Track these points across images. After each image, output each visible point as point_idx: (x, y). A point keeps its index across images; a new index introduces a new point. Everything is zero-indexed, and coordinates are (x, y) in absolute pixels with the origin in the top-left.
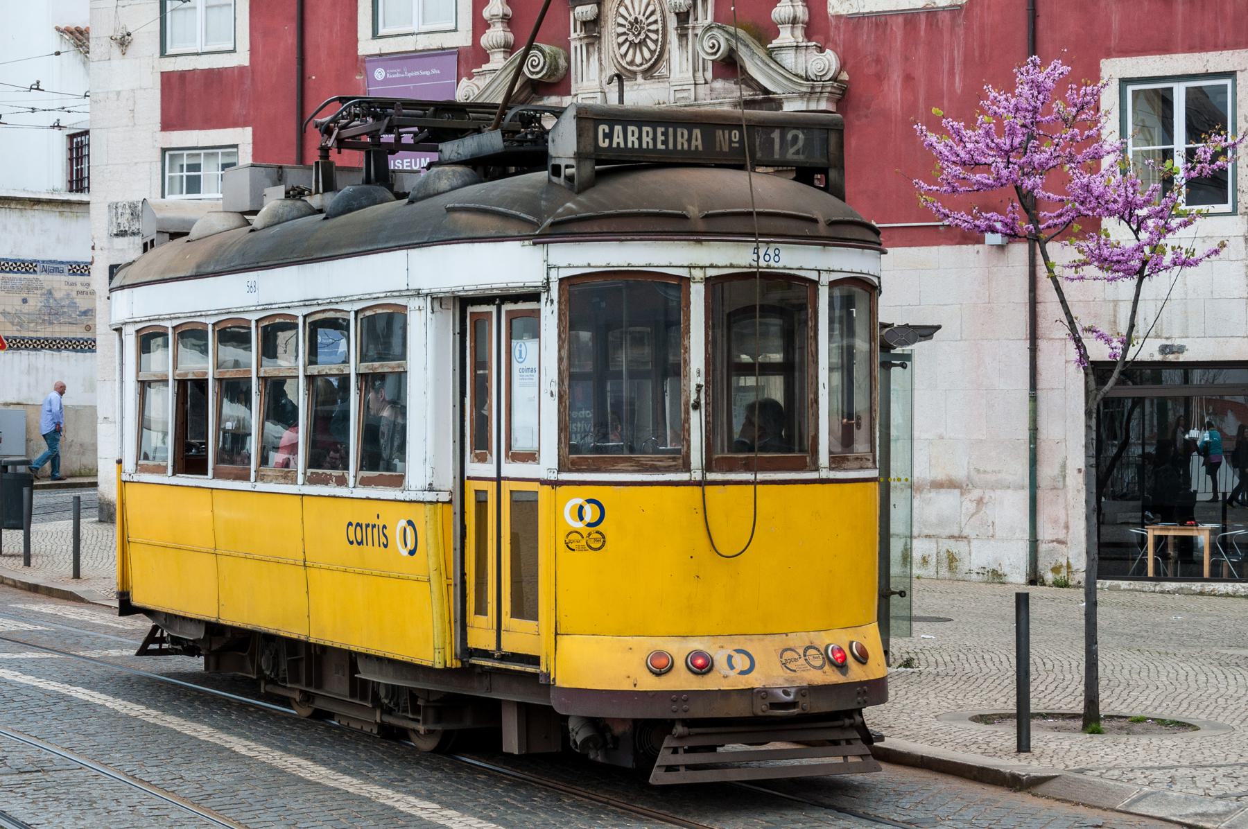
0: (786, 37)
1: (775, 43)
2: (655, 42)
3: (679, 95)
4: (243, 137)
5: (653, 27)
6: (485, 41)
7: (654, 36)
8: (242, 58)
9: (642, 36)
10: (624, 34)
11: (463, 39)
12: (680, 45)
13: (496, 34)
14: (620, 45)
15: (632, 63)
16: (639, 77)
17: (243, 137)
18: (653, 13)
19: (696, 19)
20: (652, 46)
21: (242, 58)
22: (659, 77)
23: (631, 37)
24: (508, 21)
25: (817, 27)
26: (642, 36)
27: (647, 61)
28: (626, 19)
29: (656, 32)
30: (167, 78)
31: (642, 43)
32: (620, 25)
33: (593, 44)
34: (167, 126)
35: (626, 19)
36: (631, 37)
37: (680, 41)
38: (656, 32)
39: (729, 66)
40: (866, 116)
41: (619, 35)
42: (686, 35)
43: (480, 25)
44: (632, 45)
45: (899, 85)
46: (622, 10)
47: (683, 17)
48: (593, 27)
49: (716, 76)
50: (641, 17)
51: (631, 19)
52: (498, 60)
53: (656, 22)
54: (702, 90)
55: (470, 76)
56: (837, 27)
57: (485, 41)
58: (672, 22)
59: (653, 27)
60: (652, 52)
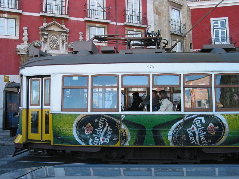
2: (58, 44)
6: (23, 39)
9: (55, 42)
11: (17, 38)
13: (25, 38)
14: (51, 43)
15: (53, 47)
18: (57, 39)
23: (53, 42)
26: (55, 42)
29: (58, 42)
32: (51, 40)
33: (46, 42)
36: (53, 42)
38: (58, 42)
41: (51, 42)
42: (64, 44)
43: (21, 36)
44: (53, 44)
46: (51, 38)
47: (63, 41)
48: (46, 40)
53: (58, 41)
57: (23, 39)
58: (61, 41)
60: (57, 45)
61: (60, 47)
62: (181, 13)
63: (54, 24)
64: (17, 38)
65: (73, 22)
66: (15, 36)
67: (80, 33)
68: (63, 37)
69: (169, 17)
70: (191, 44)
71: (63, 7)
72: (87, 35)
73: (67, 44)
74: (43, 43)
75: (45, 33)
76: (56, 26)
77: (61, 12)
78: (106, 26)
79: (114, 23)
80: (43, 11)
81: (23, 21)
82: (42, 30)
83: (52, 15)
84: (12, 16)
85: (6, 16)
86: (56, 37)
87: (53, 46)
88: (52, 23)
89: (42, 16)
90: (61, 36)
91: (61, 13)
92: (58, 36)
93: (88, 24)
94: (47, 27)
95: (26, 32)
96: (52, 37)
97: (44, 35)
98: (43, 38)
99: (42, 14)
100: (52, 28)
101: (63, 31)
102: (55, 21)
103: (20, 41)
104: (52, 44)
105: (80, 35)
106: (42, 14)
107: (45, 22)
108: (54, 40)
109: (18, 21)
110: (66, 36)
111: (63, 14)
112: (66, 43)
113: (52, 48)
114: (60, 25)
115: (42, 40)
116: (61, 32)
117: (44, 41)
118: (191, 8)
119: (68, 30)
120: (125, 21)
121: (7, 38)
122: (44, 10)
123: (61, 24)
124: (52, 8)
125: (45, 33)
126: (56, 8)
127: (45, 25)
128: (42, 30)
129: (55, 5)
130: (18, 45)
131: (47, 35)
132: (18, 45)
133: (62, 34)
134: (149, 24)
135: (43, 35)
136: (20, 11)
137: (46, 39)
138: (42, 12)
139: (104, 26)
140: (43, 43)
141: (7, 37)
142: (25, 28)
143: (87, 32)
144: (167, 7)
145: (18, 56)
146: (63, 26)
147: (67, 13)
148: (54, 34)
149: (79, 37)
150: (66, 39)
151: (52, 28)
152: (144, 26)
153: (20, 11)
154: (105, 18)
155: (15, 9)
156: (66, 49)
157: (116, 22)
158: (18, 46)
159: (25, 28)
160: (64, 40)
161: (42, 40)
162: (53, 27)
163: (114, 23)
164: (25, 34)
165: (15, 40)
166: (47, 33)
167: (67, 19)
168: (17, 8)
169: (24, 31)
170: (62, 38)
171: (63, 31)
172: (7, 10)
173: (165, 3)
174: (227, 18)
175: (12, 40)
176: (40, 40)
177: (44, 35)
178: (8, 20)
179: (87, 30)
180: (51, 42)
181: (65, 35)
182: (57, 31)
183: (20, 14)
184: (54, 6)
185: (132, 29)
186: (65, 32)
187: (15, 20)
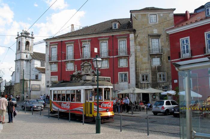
4: (57, 76)
8: (57, 71)
11: (74, 70)
13: (76, 70)
17: (57, 76)
21: (57, 71)
24: (77, 69)
30: (51, 73)
34: (51, 76)
43: (75, 69)
47: (90, 69)
48: (83, 70)
52: (76, 72)
62: (160, 41)
63: (86, 62)
64: (74, 70)
69: (149, 45)
70: (169, 58)
75: (83, 67)
78: (109, 59)
79: (112, 57)
81: (75, 63)
82: (82, 66)
85: (70, 62)
97: (82, 67)
100: (86, 64)
103: (75, 71)
118: (169, 34)
120: (117, 54)
125: (83, 67)
128: (82, 66)
134: (131, 53)
136: (74, 60)
139: (107, 59)
144: (148, 40)
151: (86, 64)
152: (128, 55)
154: (108, 55)
157: (113, 56)
163: (112, 57)
164: (76, 68)
173: (146, 37)
174: (189, 37)
177: (82, 67)
183: (74, 60)
185: (121, 58)
186: (90, 65)
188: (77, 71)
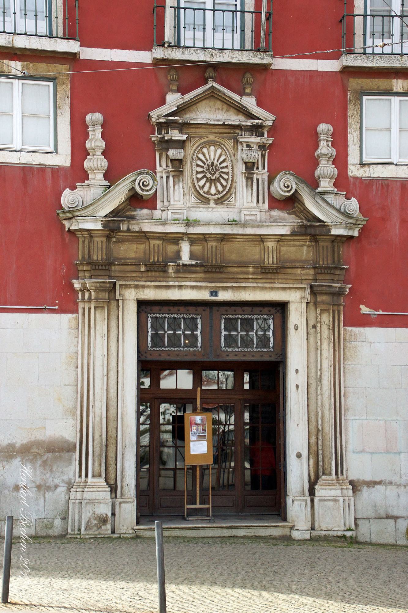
0: (325, 185)
1: (319, 189)
2: (227, 180)
3: (248, 218)
5: (225, 170)
7: (226, 176)
10: (203, 172)
12: (247, 185)
14: (199, 180)
15: (208, 193)
16: (212, 204)
18: (224, 161)
19: (257, 168)
20: (224, 183)
22: (228, 204)
23: (208, 175)
25: (343, 182)
27: (219, 193)
28: (204, 163)
29: (227, 173)
31: (218, 180)
32: (198, 166)
33: (178, 176)
35: (204, 163)
37: (247, 181)
38: (227, 173)
39: (291, 202)
40: (375, 243)
41: (197, 173)
42: (252, 179)
43: (79, 151)
45: (398, 225)
46: (201, 156)
47: (250, 167)
48: (178, 165)
49: (271, 208)
50: (215, 162)
51: (209, 162)
52: (97, 178)
53: (226, 167)
54: (264, 216)
55: (73, 188)
56: (354, 184)
58: (240, 168)
59: (225, 170)
60: (224, 187)
61: (238, 194)
63: (212, 95)
64: (63, 159)
65: (291, 79)
66: (56, 152)
67: (323, 128)
68: (250, 148)
71: (248, 16)
72: (350, 137)
73: (266, 178)
74: (168, 177)
75: (176, 135)
76: (219, 104)
77: (237, 36)
80: (166, 39)
81: (88, 88)
83: (201, 56)
84: (42, 68)
86: (219, 151)
87: (206, 189)
88: (200, 90)
89: (158, 62)
90: (240, 147)
91: (237, 46)
92: (229, 144)
93: (354, 83)
94: (182, 109)
95: (98, 135)
96: (205, 150)
98: (167, 156)
99: (159, 53)
100: (206, 114)
101: (249, 122)
102: (214, 79)
103: (77, 174)
104: (202, 183)
105: (322, 137)
106: (159, 53)
107: (175, 88)
108: (212, 164)
109: (65, 89)
110: (262, 147)
111: (248, 46)
112: (262, 174)
113: (204, 199)
114: (236, 97)
115: (162, 166)
116: (239, 127)
117: (170, 169)
119: (268, 118)
121: (23, 161)
122: (169, 35)
123: (242, 93)
124: (199, 21)
125: (176, 135)
126: (219, 22)
127: (173, 99)
128: (164, 126)
129: (214, 10)
130: (67, 191)
131: (181, 144)
132: (67, 191)
133: (246, 138)
135: (164, 146)
136: (72, 46)
137: (180, 161)
138: (161, 44)
140: (168, 177)
141: (26, 159)
142: (94, 118)
143: (350, 121)
145: (67, 238)
146: (250, 102)
147: (263, 44)
148: (212, 137)
149: (316, 146)
150: (263, 156)
153: (72, 46)
155: (51, 37)
156: (263, 203)
158: (68, 198)
159: (94, 118)
160: (254, 163)
161: (164, 165)
162: (208, 109)
164: (95, 141)
165: (56, 171)
166: (184, 137)
167: (265, 68)
168: (61, 34)
169: (90, 129)
170: (244, 154)
171: (249, 122)
172: (21, 42)
175: (42, 169)
176: (155, 167)
178: (25, 86)
179: (351, 110)
180: (197, 173)
181: (254, 140)
182: (224, 125)
183: (71, 58)
184: (209, 14)
186: (256, 130)
187: (51, 84)
188: (112, 176)
